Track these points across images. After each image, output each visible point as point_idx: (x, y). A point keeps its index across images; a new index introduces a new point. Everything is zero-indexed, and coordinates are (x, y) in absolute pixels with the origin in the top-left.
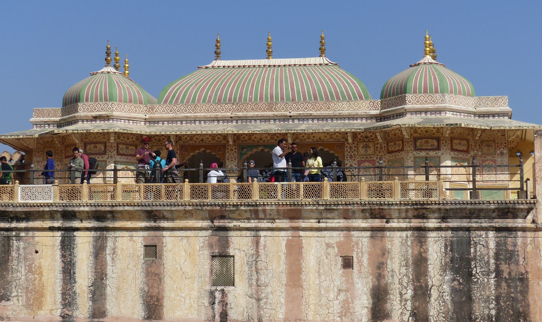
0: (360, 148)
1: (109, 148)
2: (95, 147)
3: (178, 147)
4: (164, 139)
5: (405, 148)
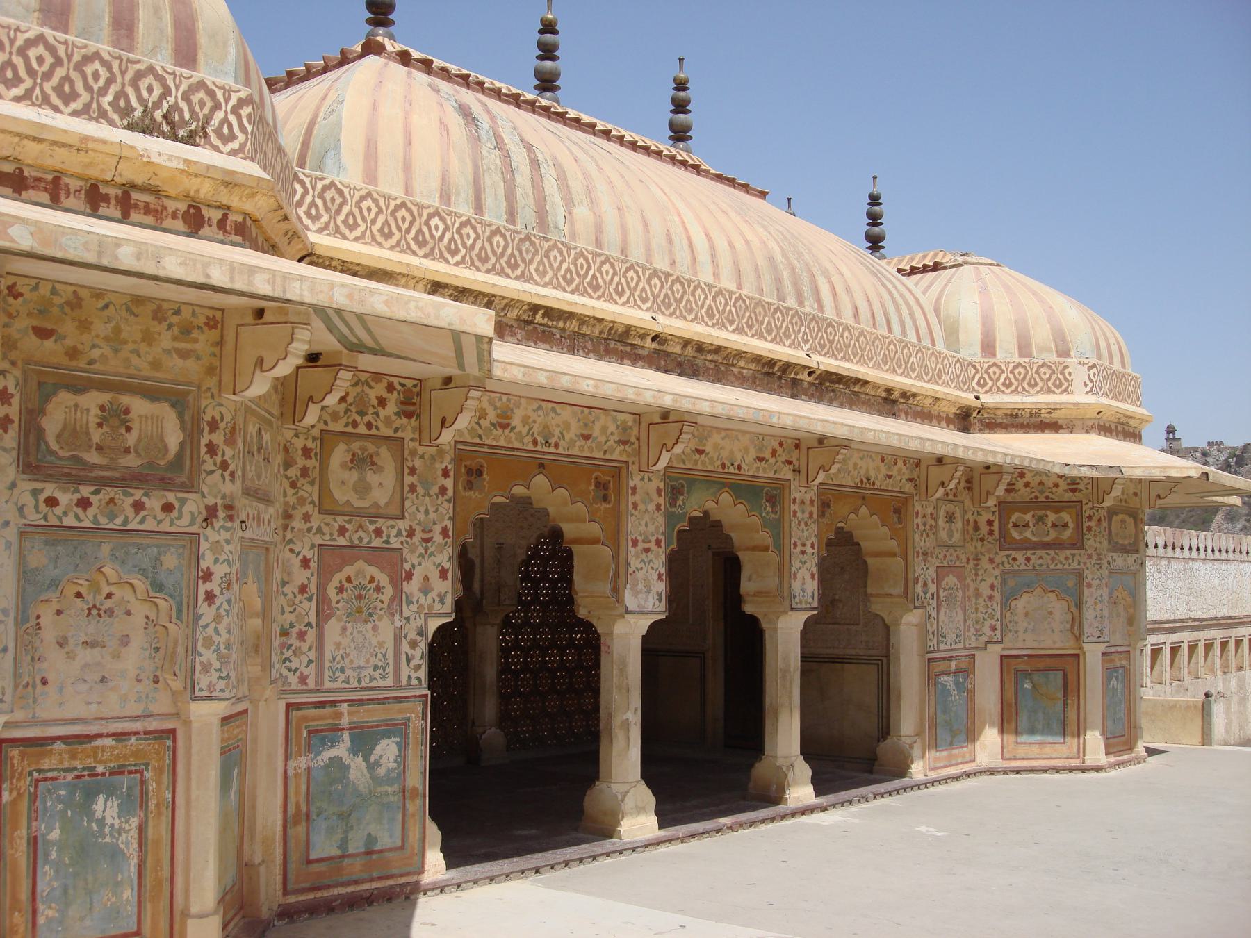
0: (941, 522)
1: (218, 438)
2: (116, 417)
3: (447, 462)
4: (382, 402)
5: (1089, 542)
